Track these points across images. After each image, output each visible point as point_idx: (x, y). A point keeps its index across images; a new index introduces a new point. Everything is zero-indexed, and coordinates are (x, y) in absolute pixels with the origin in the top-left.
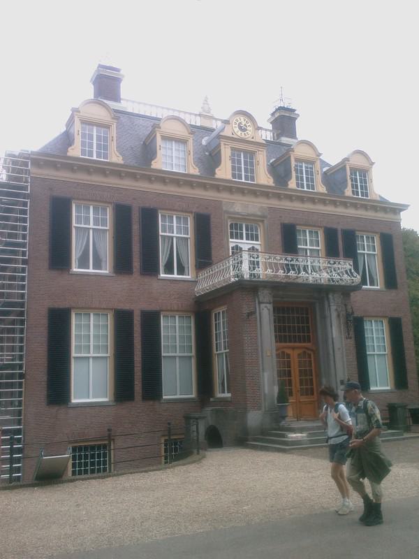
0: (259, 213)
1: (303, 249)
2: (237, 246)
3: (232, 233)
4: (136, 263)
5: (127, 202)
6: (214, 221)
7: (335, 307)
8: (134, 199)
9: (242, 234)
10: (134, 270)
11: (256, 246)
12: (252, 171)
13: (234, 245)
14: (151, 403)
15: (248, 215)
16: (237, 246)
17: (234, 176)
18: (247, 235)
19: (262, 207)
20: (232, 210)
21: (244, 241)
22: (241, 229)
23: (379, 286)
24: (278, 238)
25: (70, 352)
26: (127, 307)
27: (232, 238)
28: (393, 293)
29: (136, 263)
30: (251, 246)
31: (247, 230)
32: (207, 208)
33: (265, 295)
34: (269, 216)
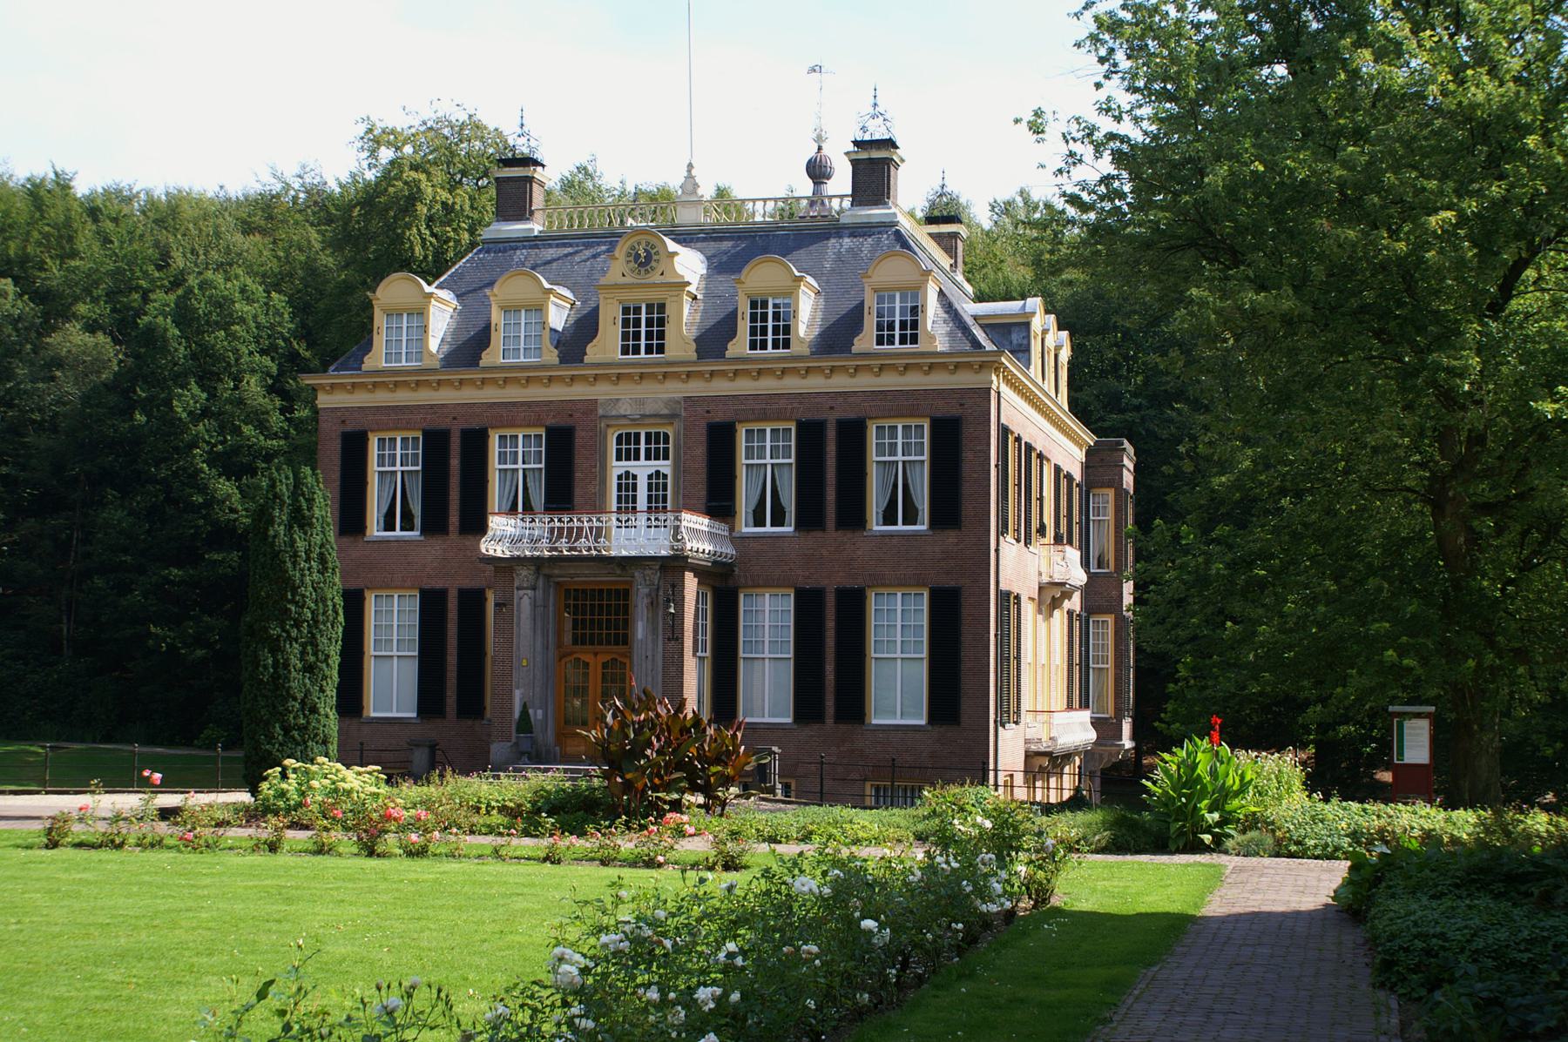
0: (666, 411)
1: (760, 465)
2: (627, 473)
3: (619, 452)
4: (454, 519)
5: (441, 424)
6: (580, 437)
7: (646, 590)
8: (454, 418)
9: (637, 451)
10: (451, 528)
11: (663, 470)
12: (661, 335)
13: (622, 471)
14: (470, 722)
15: (644, 416)
16: (627, 473)
17: (625, 351)
18: (648, 451)
19: (670, 400)
20: (614, 413)
21: (643, 461)
22: (637, 442)
23: (922, 527)
24: (700, 451)
25: (366, 649)
26: (438, 584)
27: (619, 458)
28: (950, 537)
29: (454, 519)
30: (653, 470)
31: (648, 442)
32: (571, 415)
33: (524, 574)
34: (683, 414)
